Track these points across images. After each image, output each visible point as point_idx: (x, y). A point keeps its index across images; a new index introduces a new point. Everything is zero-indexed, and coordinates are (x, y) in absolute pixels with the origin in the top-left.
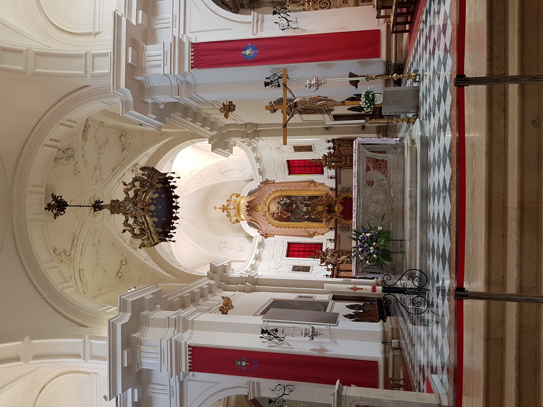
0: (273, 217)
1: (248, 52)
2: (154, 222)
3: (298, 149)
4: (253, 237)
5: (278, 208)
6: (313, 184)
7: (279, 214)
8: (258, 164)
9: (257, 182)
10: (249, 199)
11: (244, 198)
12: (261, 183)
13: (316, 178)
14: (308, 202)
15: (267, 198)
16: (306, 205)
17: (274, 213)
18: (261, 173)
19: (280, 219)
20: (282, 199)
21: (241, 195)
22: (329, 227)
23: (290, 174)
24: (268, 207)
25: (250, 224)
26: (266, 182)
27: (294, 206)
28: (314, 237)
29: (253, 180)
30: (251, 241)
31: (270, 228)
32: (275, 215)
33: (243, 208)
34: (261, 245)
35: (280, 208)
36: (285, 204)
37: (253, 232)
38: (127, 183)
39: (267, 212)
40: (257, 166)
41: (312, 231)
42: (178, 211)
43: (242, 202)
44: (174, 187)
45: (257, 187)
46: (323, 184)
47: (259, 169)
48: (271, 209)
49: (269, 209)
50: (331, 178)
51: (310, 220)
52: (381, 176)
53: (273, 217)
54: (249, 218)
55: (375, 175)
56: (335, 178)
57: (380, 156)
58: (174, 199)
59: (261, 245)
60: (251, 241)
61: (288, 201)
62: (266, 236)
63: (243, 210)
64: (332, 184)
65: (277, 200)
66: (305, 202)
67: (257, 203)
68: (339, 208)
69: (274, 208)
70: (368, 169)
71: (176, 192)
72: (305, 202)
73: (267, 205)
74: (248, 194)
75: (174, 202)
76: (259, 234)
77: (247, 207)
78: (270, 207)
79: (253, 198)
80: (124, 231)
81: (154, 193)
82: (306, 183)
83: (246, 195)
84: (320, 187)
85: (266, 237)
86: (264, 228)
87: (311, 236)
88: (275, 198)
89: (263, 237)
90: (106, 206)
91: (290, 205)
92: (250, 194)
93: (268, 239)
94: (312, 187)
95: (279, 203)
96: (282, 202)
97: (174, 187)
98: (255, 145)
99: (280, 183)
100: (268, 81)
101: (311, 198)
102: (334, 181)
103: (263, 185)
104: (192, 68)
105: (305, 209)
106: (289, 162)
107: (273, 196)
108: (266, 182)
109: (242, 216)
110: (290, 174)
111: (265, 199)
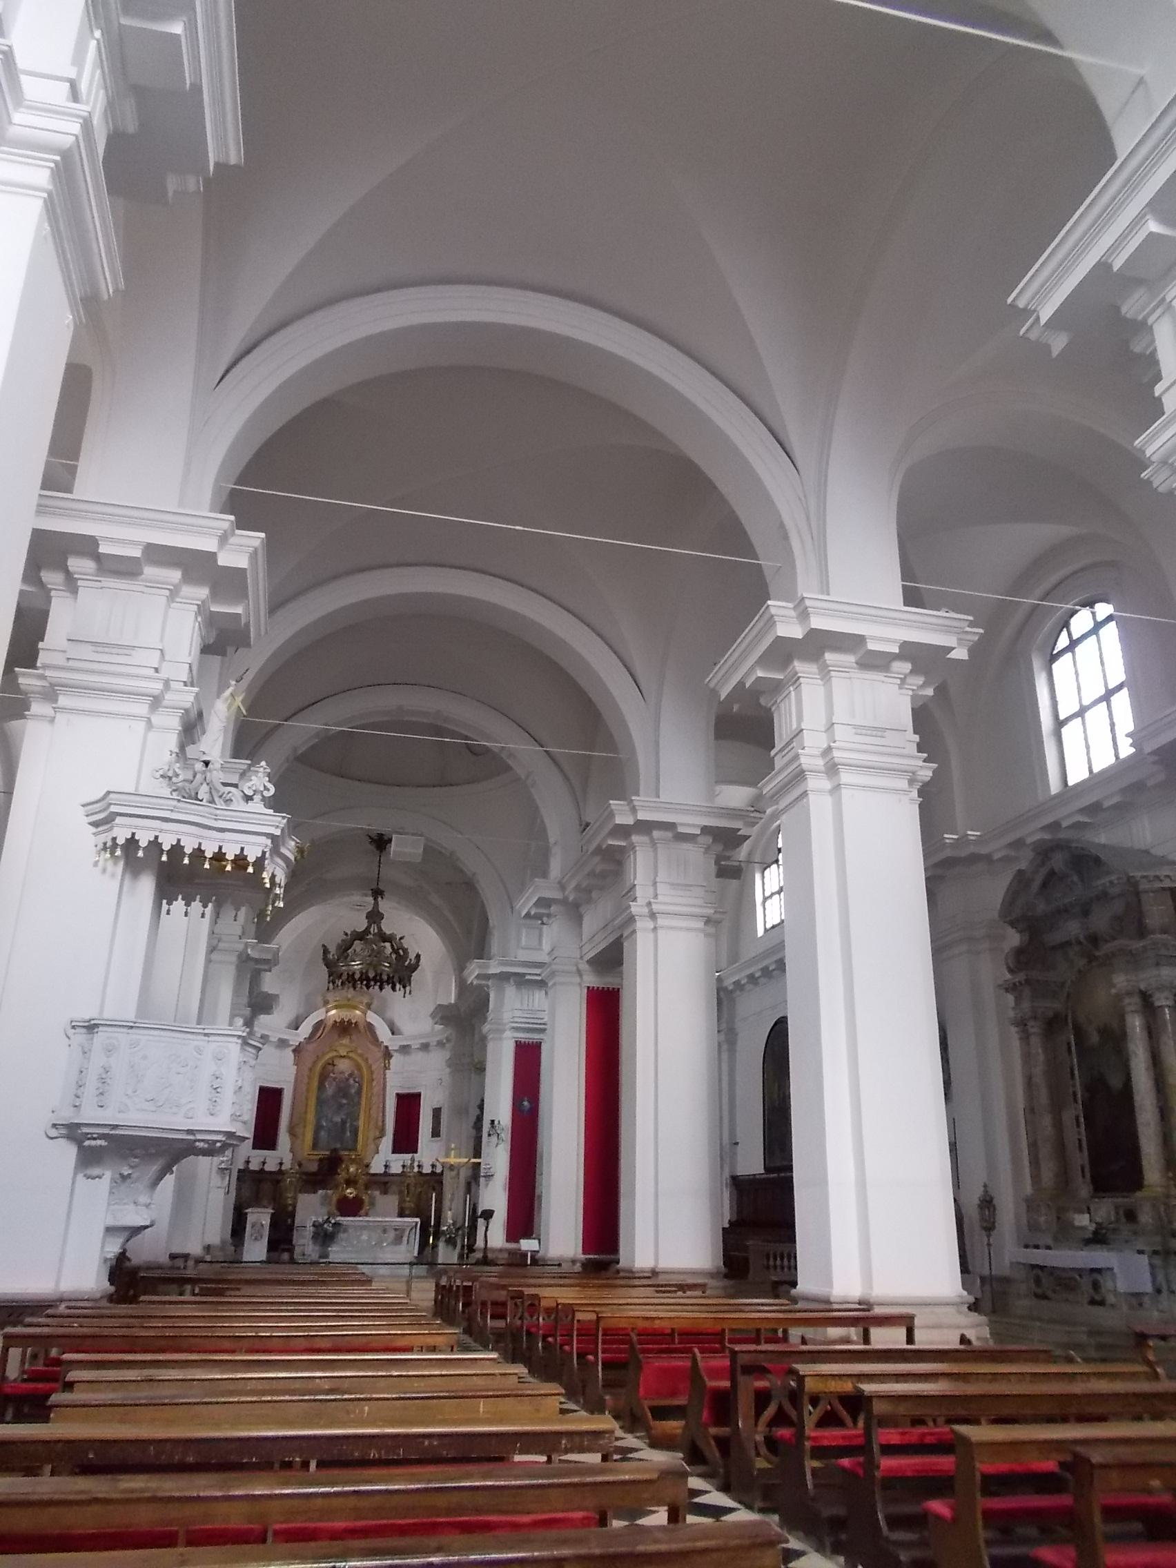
0: (329, 1064)
1: (526, 1103)
2: (354, 974)
3: (437, 1113)
4: (297, 1029)
5: (342, 1073)
6: (378, 1134)
7: (331, 1075)
8: (418, 1046)
9: (390, 1040)
10: (361, 1027)
11: (363, 1016)
12: (387, 1047)
13: (387, 1142)
14: (348, 1125)
15: (361, 1055)
16: (344, 1122)
17: (334, 1065)
18: (405, 1049)
19: (323, 1077)
20: (357, 1080)
21: (370, 1013)
22: (303, 1162)
23: (400, 1097)
24: (344, 1057)
25: (318, 1026)
26: (387, 1054)
27: (344, 1101)
28: (287, 1135)
29: (393, 1034)
30: (288, 1027)
31: (308, 1059)
32: (330, 1067)
33: (346, 1015)
34: (282, 1043)
35: (342, 1076)
36: (349, 1086)
37: (306, 1029)
38: (402, 941)
39: (335, 1054)
40: (415, 1044)
41: (299, 1130)
42: (364, 987)
43: (358, 1012)
44: (394, 989)
45: (380, 1040)
46: (377, 1152)
47: (408, 1046)
48: (343, 1060)
49: (341, 1056)
50: (386, 1166)
51: (318, 1128)
52: (390, 1240)
53: (329, 1064)
54: (330, 1023)
55: (391, 1235)
56: (385, 1172)
57: (405, 1239)
58: (378, 984)
59: (282, 1043)
60: (288, 1027)
61: (353, 1091)
62: (297, 1051)
63: (346, 1013)
64: (377, 1167)
65: (356, 1072)
66: (349, 1120)
67: (354, 1037)
68: (351, 1193)
69: (344, 1066)
70: (396, 1230)
71: (388, 988)
72: (349, 1120)
73: (351, 1054)
74: (370, 1023)
75: (376, 983)
76: (302, 1040)
77: (350, 1022)
78: (346, 1061)
79: (363, 1031)
80: (346, 934)
81: (388, 975)
82: (380, 1123)
83: (368, 1020)
84: (372, 1147)
85: (294, 1051)
86: (311, 1047)
87: (292, 1132)
88: (359, 1067)
89: (294, 1047)
90: (376, 904)
91: (345, 1096)
92: (370, 1027)
93: (291, 1055)
94: (373, 1133)
95: (351, 1075)
96: (351, 1081)
97: (394, 989)
98: (447, 1045)
99: (385, 1079)
100: (496, 1123)
101: (355, 1132)
102: (381, 1170)
103: (382, 1048)
104: (516, 1042)
105: (338, 1119)
106: (419, 1095)
107: (363, 1064)
108: (387, 1054)
109: (333, 1012)
110: (400, 1097)
111: (359, 1051)
